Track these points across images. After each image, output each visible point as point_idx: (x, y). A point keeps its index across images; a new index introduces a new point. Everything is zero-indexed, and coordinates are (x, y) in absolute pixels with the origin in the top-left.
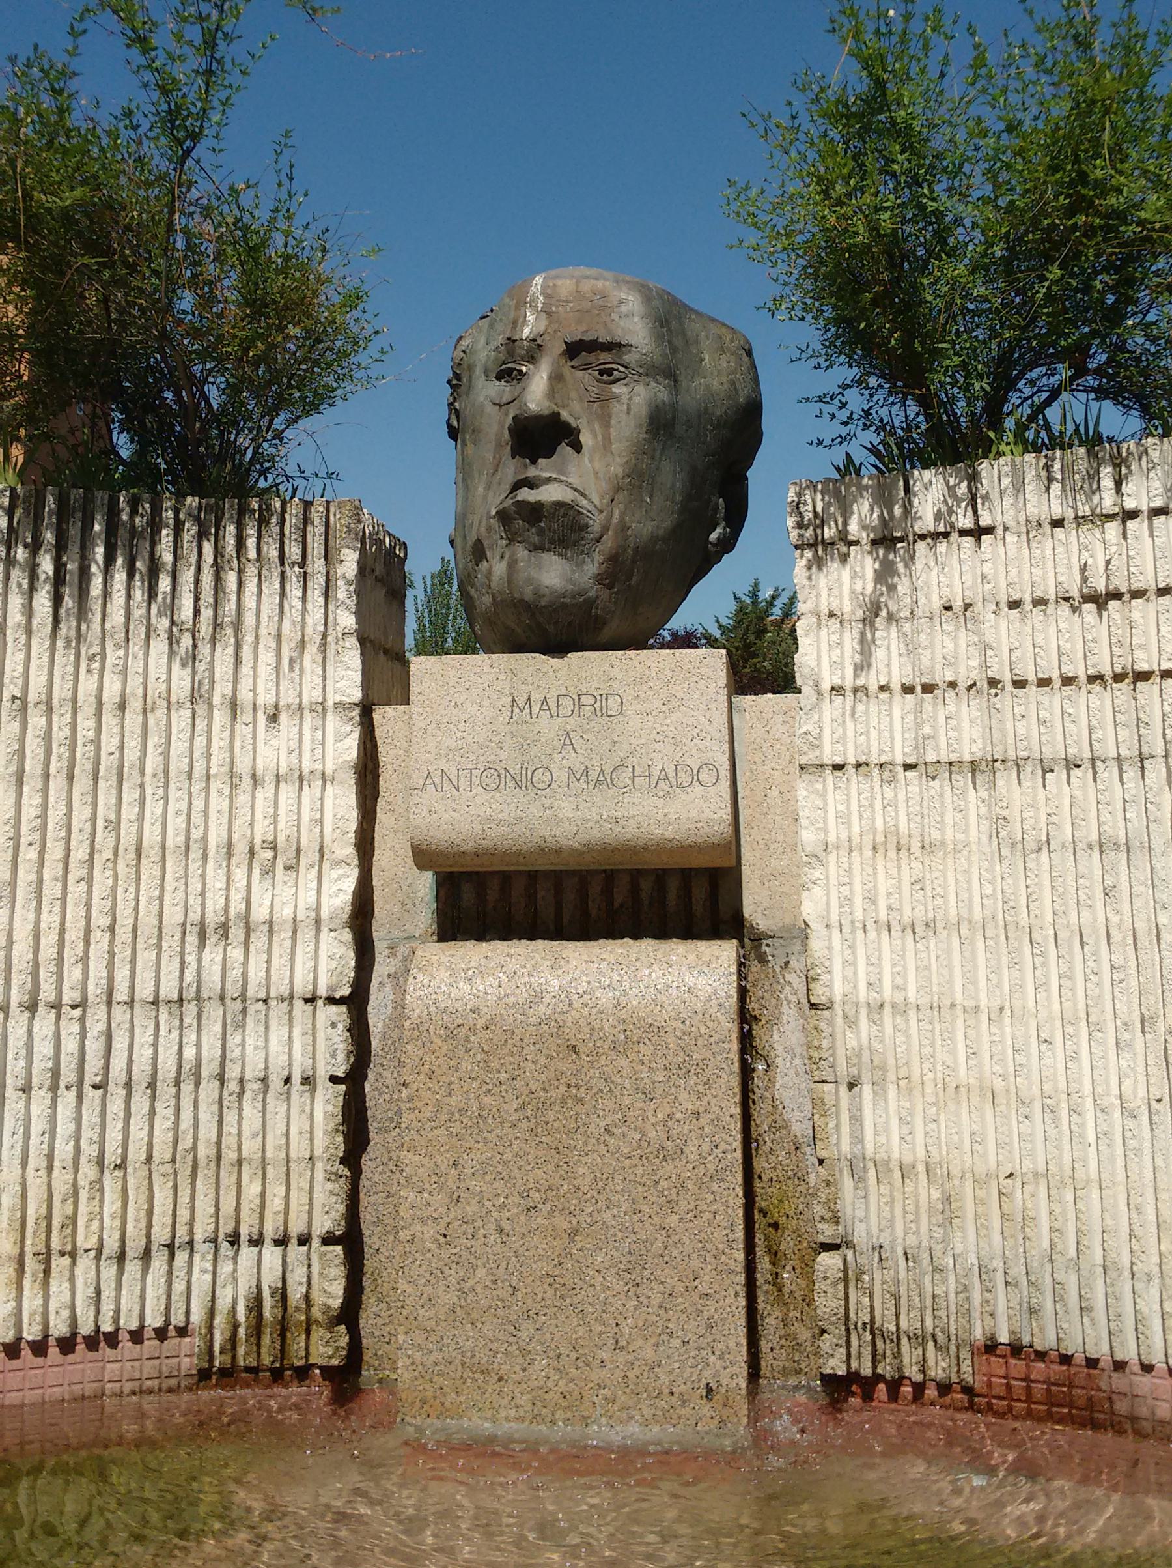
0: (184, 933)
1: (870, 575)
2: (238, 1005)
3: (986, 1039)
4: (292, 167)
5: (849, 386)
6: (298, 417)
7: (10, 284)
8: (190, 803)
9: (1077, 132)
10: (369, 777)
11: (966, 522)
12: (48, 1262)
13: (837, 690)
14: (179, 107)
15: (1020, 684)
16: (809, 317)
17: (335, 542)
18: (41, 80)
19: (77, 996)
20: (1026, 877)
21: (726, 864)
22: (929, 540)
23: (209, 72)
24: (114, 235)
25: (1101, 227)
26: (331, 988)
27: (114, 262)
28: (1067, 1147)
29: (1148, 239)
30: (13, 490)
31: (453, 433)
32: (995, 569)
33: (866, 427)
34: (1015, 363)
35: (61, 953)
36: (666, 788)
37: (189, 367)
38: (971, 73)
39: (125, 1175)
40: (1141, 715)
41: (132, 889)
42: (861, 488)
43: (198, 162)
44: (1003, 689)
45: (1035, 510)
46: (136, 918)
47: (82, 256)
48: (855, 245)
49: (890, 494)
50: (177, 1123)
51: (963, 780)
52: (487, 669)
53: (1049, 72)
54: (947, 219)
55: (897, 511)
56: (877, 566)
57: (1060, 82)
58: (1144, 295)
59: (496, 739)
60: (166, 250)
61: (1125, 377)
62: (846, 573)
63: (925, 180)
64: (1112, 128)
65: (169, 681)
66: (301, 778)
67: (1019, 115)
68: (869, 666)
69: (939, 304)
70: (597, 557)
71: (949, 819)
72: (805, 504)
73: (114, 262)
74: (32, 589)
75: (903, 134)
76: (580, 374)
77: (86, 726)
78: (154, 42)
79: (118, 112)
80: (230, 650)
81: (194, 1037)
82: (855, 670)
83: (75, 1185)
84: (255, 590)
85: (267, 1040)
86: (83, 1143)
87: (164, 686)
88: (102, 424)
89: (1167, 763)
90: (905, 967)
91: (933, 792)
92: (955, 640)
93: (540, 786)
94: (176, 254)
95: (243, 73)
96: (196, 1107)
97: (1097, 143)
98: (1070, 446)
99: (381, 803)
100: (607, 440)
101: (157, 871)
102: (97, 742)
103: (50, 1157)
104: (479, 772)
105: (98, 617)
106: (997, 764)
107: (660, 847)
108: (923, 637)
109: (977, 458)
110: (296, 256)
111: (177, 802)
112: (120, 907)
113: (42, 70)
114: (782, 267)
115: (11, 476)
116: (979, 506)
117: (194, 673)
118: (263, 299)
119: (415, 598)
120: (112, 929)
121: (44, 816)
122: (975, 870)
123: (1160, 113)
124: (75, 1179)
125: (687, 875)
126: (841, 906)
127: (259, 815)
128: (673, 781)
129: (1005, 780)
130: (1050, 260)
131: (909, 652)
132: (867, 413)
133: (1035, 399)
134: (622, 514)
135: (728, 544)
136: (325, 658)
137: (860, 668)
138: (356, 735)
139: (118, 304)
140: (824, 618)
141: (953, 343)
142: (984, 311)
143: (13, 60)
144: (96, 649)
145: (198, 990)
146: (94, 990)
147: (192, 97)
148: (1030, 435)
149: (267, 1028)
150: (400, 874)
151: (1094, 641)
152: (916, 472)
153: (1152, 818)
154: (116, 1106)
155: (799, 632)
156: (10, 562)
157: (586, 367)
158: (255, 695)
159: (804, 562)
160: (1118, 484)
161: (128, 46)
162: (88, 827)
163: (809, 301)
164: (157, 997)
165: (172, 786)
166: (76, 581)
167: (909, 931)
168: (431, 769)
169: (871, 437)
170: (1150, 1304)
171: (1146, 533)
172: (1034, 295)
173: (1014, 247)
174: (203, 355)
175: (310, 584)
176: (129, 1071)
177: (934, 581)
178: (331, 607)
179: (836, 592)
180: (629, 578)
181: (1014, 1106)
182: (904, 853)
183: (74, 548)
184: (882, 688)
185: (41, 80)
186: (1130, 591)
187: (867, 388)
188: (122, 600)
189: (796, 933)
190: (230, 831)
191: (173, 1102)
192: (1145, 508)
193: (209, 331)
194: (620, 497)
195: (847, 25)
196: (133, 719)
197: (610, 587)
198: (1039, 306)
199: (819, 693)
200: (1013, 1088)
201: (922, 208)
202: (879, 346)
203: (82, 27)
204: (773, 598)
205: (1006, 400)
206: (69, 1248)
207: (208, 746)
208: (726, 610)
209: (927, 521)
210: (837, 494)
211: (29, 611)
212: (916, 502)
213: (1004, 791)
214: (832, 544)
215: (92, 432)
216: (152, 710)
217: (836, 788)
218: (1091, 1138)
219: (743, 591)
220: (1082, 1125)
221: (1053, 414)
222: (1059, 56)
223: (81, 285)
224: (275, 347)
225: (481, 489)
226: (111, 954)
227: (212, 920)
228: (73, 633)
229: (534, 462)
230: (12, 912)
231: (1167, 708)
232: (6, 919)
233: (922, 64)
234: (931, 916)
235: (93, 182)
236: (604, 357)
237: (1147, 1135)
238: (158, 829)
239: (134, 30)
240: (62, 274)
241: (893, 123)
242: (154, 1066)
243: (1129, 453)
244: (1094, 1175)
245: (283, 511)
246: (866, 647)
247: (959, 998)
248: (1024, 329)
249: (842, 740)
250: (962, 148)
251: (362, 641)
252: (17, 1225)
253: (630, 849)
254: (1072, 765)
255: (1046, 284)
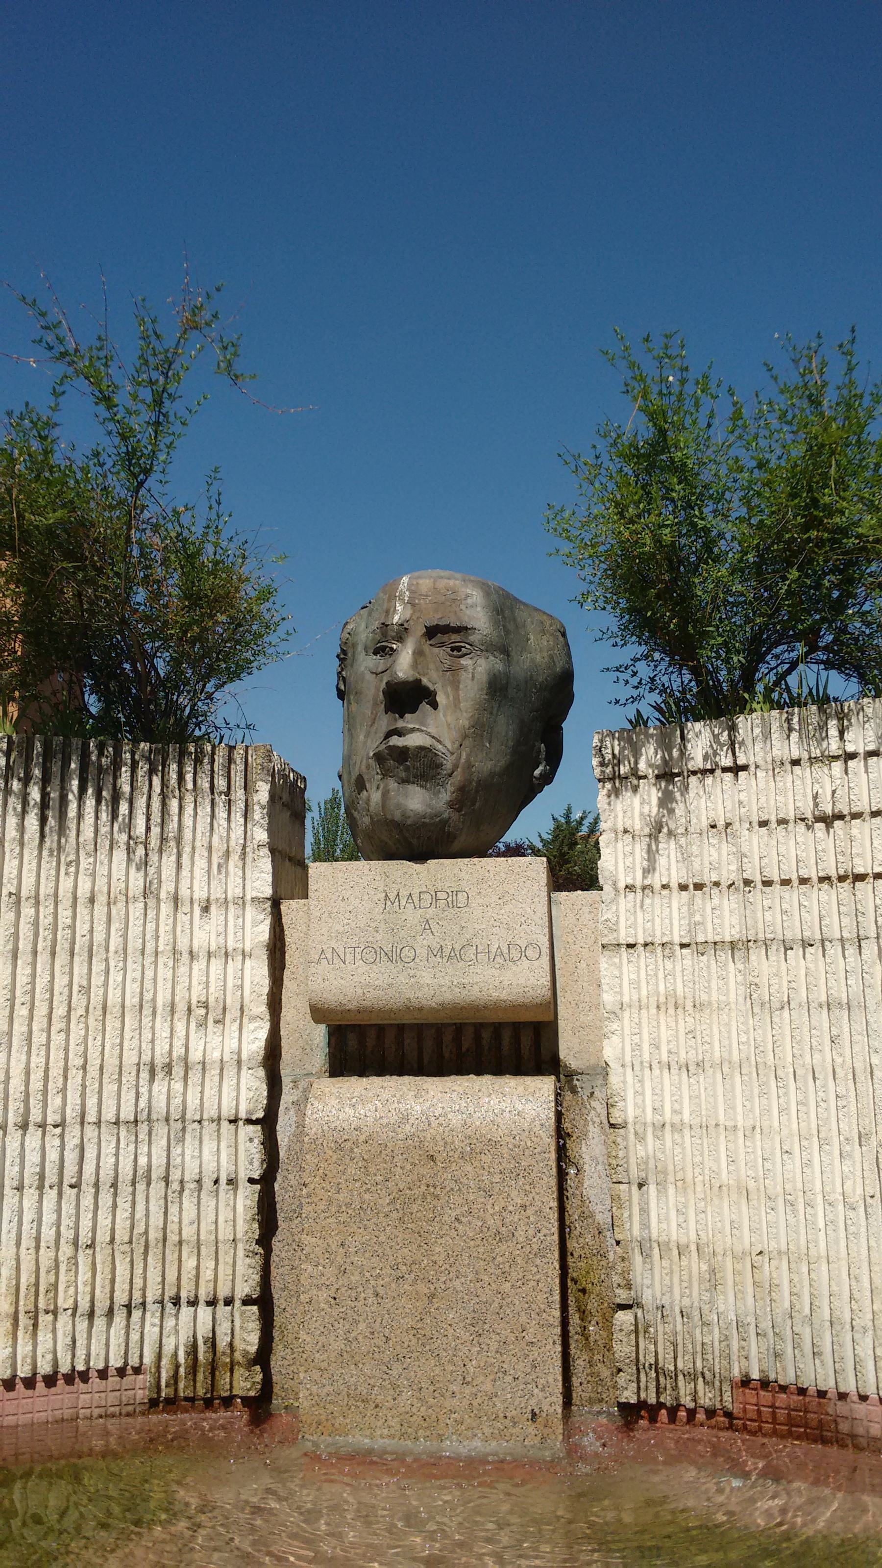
0: (138, 1071)
1: (655, 801)
2: (179, 1125)
3: (742, 1151)
4: (219, 494)
5: (639, 660)
6: (225, 683)
7: (7, 582)
8: (143, 973)
9: (811, 468)
10: (278, 954)
11: (727, 762)
12: (36, 1318)
13: (630, 888)
14: (135, 450)
15: (767, 883)
16: (609, 607)
17: (253, 777)
18: (31, 429)
19: (58, 1118)
20: (772, 1028)
21: (546, 1019)
22: (699, 775)
23: (158, 423)
24: (85, 545)
25: (829, 540)
26: (249, 1112)
27: (86, 566)
28: (803, 1231)
29: (864, 549)
30: (10, 738)
31: (341, 695)
32: (749, 797)
33: (651, 690)
34: (764, 642)
35: (46, 1086)
36: (501, 961)
37: (142, 645)
38: (730, 424)
39: (94, 1253)
40: (859, 907)
41: (99, 1038)
42: (648, 736)
43: (149, 491)
44: (755, 887)
45: (779, 753)
46: (103, 1060)
47: (62, 561)
48: (644, 553)
49: (670, 740)
50: (133, 1214)
51: (725, 956)
52: (366, 872)
53: (790, 423)
54: (713, 534)
55: (675, 753)
56: (660, 794)
57: (798, 431)
58: (861, 591)
59: (373, 925)
60: (125, 557)
61: (846, 653)
62: (637, 800)
63: (696, 504)
64: (837, 465)
65: (127, 881)
66: (226, 954)
67: (767, 456)
68: (654, 869)
69: (707, 597)
70: (450, 788)
71: (714, 985)
72: (606, 748)
73: (86, 566)
74: (24, 812)
75: (680, 469)
76: (436, 650)
77: (65, 915)
78: (116, 400)
79: (89, 453)
80: (173, 858)
81: (146, 1149)
82: (644, 873)
83: (56, 1260)
84: (192, 813)
85: (201, 1152)
86: (63, 1229)
87: (124, 885)
88: (77, 688)
89: (878, 943)
90: (681, 1097)
91: (702, 965)
92: (719, 850)
93: (407, 960)
94: (133, 560)
95: (183, 424)
96: (147, 1202)
97: (825, 476)
98: (806, 705)
99: (287, 973)
100: (457, 701)
101: (118, 1024)
102: (73, 927)
103: (38, 1239)
104: (360, 950)
105: (73, 833)
106: (750, 944)
107: (497, 1006)
108: (694, 848)
109: (735, 713)
110: (223, 562)
111: (133, 972)
112: (90, 1051)
113: (32, 422)
114: (588, 570)
115: (8, 727)
116: (737, 750)
117: (146, 875)
118: (198, 593)
119: (312, 819)
120: (84, 1068)
121: (33, 983)
122: (734, 1023)
123: (873, 454)
124: (57, 1256)
125: (517, 1027)
126: (633, 1051)
127: (195, 982)
128: (507, 956)
129: (756, 955)
130: (790, 565)
131: (684, 860)
132: (652, 680)
133: (779, 669)
134: (468, 756)
135: (548, 778)
136: (244, 864)
137: (648, 871)
138: (268, 921)
139: (89, 597)
140: (620, 834)
141: (717, 627)
142: (741, 603)
143: (10, 414)
144: (72, 857)
145: (149, 1114)
146: (71, 1114)
147: (144, 442)
148: (775, 696)
149: (201, 1142)
150: (301, 1026)
151: (824, 851)
152: (689, 724)
153: (867, 984)
154: (87, 1201)
155: (602, 844)
156: (7, 791)
157: (441, 645)
158: (192, 892)
159: (605, 792)
160: (841, 733)
161: (97, 404)
162: (66, 991)
163: (609, 596)
164: (118, 1118)
165: (130, 960)
166: (57, 805)
167: (684, 1069)
168: (325, 947)
169: (655, 698)
170: (865, 1350)
171: (863, 769)
172: (778, 591)
173: (763, 555)
174: (153, 636)
175: (233, 808)
176: (97, 1174)
177: (703, 806)
178: (249, 826)
179: (629, 814)
180: (474, 804)
181: (763, 1201)
182: (680, 1011)
183: (56, 781)
184: (664, 887)
185: (31, 429)
186: (850, 814)
187: (652, 661)
188: (92, 821)
189: (599, 1070)
190: (173, 994)
191: (130, 1198)
192: (861, 751)
193: (157, 618)
194: (467, 743)
195: (638, 388)
196: (100, 910)
197: (459, 810)
198: (782, 599)
199: (617, 890)
200: (762, 1187)
201: (694, 525)
202: (661, 629)
203: (62, 389)
204: (582, 818)
205: (757, 670)
206: (52, 1307)
207: (157, 930)
208: (546, 828)
209: (697, 762)
210: (630, 740)
211: (21, 829)
212: (689, 746)
213: (755, 964)
214: (626, 778)
215: (69, 693)
216: (115, 903)
217: (629, 962)
218: (821, 1225)
219: (559, 814)
220: (815, 1215)
221: (792, 680)
222: (797, 411)
223: (61, 584)
224: (207, 630)
225: (362, 737)
226: (84, 1086)
227: (159, 1061)
228: (55, 845)
229: (402, 717)
230: (9, 1055)
231: (878, 902)
232: (4, 1060)
233: (694, 417)
234: (700, 1058)
235: (70, 506)
236: (455, 637)
237: (863, 1222)
238: (119, 992)
239: (101, 392)
240: (46, 575)
241: (672, 461)
242: (116, 1171)
243: (850, 710)
244: (823, 1253)
245: (213, 753)
246: (651, 855)
247: (722, 1119)
248: (770, 616)
249: (634, 925)
250: (724, 480)
251: (273, 851)
252: (13, 1290)
253: (474, 1008)
254: (807, 944)
255: (787, 582)
